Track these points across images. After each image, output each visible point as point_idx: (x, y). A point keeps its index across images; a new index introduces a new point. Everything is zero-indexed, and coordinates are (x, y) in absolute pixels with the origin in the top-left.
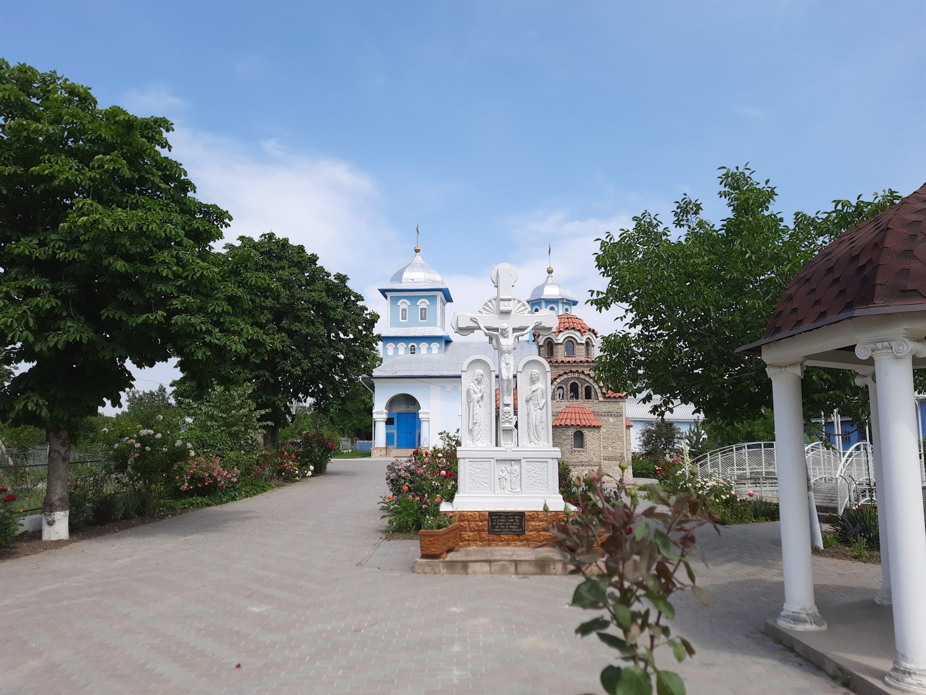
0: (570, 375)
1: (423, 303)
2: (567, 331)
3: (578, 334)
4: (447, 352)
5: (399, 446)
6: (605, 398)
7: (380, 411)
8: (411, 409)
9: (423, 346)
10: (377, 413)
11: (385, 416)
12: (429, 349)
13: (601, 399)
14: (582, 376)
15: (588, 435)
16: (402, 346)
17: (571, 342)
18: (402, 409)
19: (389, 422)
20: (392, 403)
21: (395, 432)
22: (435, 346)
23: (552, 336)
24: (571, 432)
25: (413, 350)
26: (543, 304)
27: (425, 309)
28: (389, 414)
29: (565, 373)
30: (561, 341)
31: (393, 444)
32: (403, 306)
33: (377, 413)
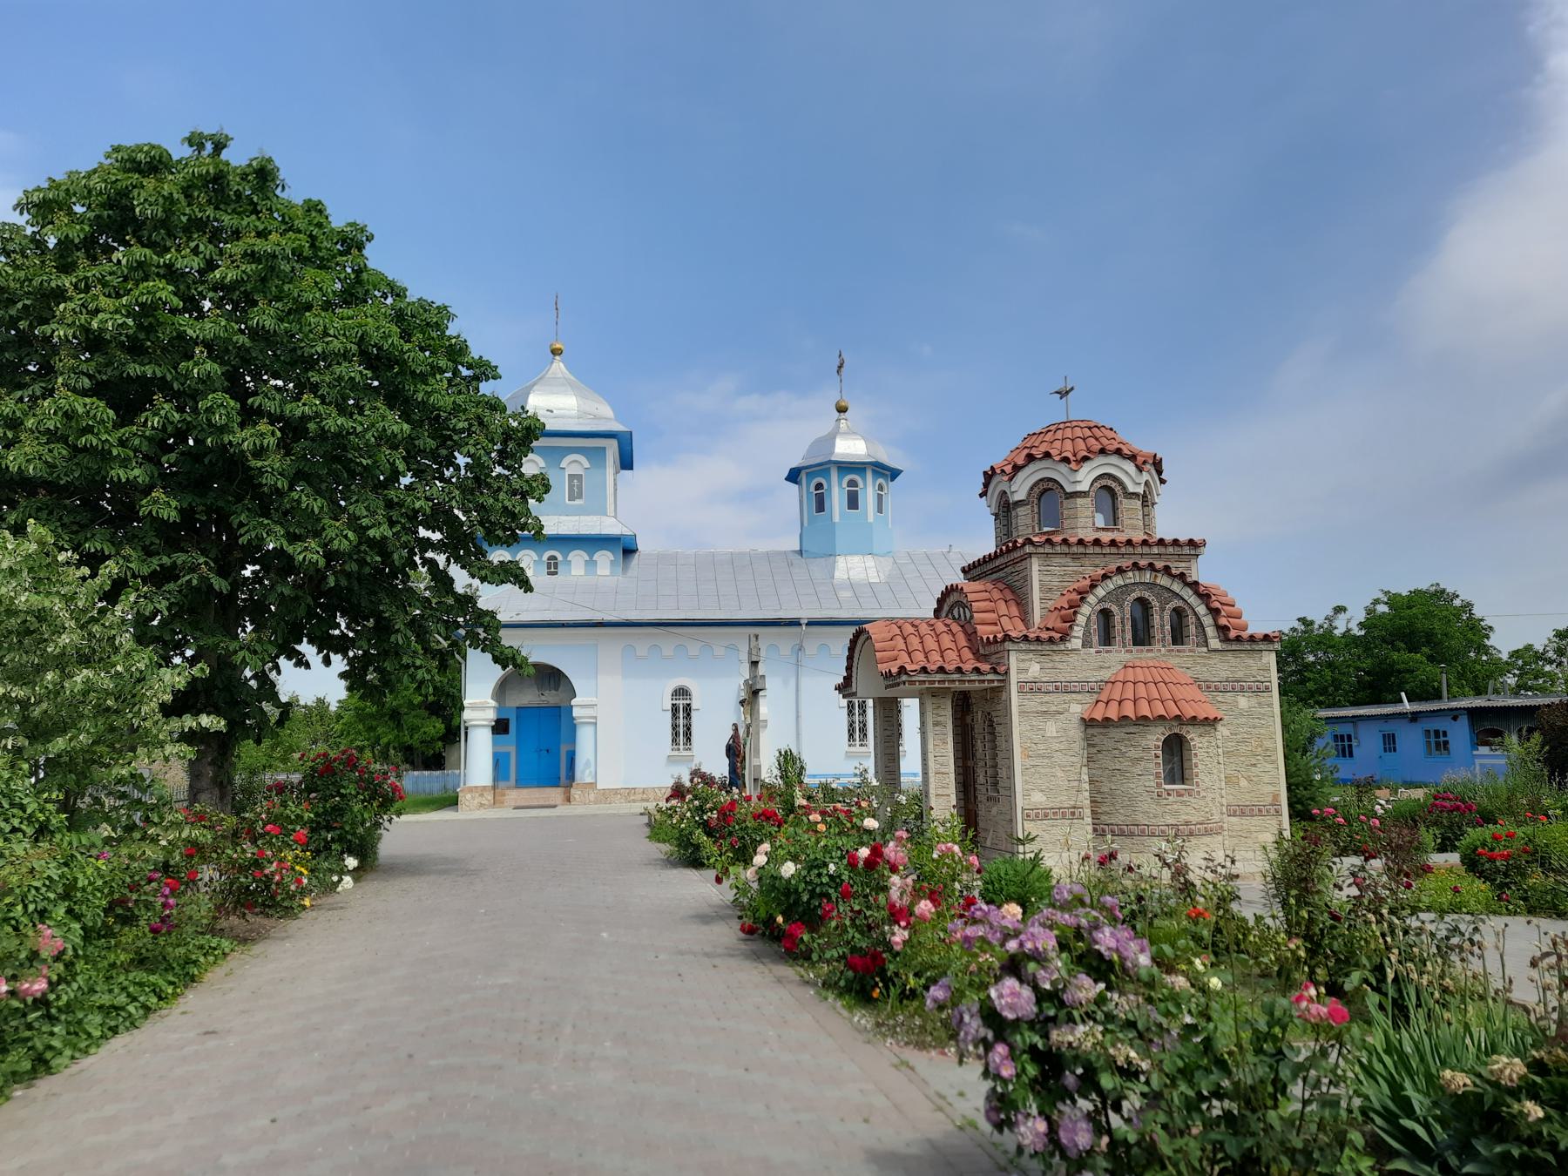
0: (1132, 577)
2: (1101, 460)
3: (1130, 467)
4: (630, 573)
5: (520, 784)
6: (1226, 640)
8: (551, 698)
9: (577, 557)
10: (474, 707)
11: (491, 715)
12: (591, 564)
13: (1215, 643)
14: (1163, 581)
15: (1197, 740)
17: (1109, 491)
19: (500, 727)
21: (512, 749)
22: (604, 558)
23: (1060, 473)
24: (1154, 738)
27: (579, 477)
28: (498, 710)
29: (1120, 571)
30: (1084, 487)
31: (507, 778)
33: (474, 707)
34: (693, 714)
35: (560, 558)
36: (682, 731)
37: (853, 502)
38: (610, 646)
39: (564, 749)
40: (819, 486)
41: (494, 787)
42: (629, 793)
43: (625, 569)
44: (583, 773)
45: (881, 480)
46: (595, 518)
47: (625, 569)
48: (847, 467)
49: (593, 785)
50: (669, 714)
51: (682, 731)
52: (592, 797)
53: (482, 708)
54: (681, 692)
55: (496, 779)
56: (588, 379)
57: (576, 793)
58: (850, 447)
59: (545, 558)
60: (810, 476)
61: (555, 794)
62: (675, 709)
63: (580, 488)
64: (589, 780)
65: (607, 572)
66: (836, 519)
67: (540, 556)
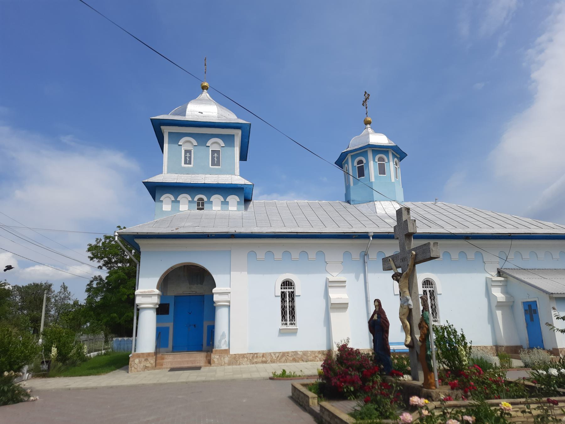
1: (215, 144)
4: (248, 210)
5: (176, 349)
7: (147, 290)
8: (197, 289)
9: (217, 199)
10: (143, 295)
11: (156, 300)
12: (225, 203)
16: (184, 198)
18: (183, 289)
19: (162, 310)
20: (166, 282)
21: (170, 325)
22: (233, 199)
25: (201, 205)
26: (370, 155)
28: (162, 297)
31: (166, 346)
32: (189, 147)
33: (143, 295)
34: (296, 299)
36: (288, 312)
37: (382, 170)
38: (239, 253)
39: (206, 324)
40: (360, 162)
41: (156, 353)
42: (253, 358)
43: (246, 208)
44: (220, 343)
45: (396, 159)
46: (228, 176)
47: (246, 208)
48: (378, 150)
49: (227, 351)
50: (279, 299)
51: (288, 312)
52: (227, 359)
53: (150, 295)
54: (287, 284)
55: (157, 347)
56: (221, 98)
57: (215, 357)
58: (379, 139)
59: (196, 199)
60: (353, 157)
61: (199, 358)
62: (283, 295)
63: (218, 158)
64: (224, 347)
65: (235, 209)
66: (373, 179)
67: (193, 198)
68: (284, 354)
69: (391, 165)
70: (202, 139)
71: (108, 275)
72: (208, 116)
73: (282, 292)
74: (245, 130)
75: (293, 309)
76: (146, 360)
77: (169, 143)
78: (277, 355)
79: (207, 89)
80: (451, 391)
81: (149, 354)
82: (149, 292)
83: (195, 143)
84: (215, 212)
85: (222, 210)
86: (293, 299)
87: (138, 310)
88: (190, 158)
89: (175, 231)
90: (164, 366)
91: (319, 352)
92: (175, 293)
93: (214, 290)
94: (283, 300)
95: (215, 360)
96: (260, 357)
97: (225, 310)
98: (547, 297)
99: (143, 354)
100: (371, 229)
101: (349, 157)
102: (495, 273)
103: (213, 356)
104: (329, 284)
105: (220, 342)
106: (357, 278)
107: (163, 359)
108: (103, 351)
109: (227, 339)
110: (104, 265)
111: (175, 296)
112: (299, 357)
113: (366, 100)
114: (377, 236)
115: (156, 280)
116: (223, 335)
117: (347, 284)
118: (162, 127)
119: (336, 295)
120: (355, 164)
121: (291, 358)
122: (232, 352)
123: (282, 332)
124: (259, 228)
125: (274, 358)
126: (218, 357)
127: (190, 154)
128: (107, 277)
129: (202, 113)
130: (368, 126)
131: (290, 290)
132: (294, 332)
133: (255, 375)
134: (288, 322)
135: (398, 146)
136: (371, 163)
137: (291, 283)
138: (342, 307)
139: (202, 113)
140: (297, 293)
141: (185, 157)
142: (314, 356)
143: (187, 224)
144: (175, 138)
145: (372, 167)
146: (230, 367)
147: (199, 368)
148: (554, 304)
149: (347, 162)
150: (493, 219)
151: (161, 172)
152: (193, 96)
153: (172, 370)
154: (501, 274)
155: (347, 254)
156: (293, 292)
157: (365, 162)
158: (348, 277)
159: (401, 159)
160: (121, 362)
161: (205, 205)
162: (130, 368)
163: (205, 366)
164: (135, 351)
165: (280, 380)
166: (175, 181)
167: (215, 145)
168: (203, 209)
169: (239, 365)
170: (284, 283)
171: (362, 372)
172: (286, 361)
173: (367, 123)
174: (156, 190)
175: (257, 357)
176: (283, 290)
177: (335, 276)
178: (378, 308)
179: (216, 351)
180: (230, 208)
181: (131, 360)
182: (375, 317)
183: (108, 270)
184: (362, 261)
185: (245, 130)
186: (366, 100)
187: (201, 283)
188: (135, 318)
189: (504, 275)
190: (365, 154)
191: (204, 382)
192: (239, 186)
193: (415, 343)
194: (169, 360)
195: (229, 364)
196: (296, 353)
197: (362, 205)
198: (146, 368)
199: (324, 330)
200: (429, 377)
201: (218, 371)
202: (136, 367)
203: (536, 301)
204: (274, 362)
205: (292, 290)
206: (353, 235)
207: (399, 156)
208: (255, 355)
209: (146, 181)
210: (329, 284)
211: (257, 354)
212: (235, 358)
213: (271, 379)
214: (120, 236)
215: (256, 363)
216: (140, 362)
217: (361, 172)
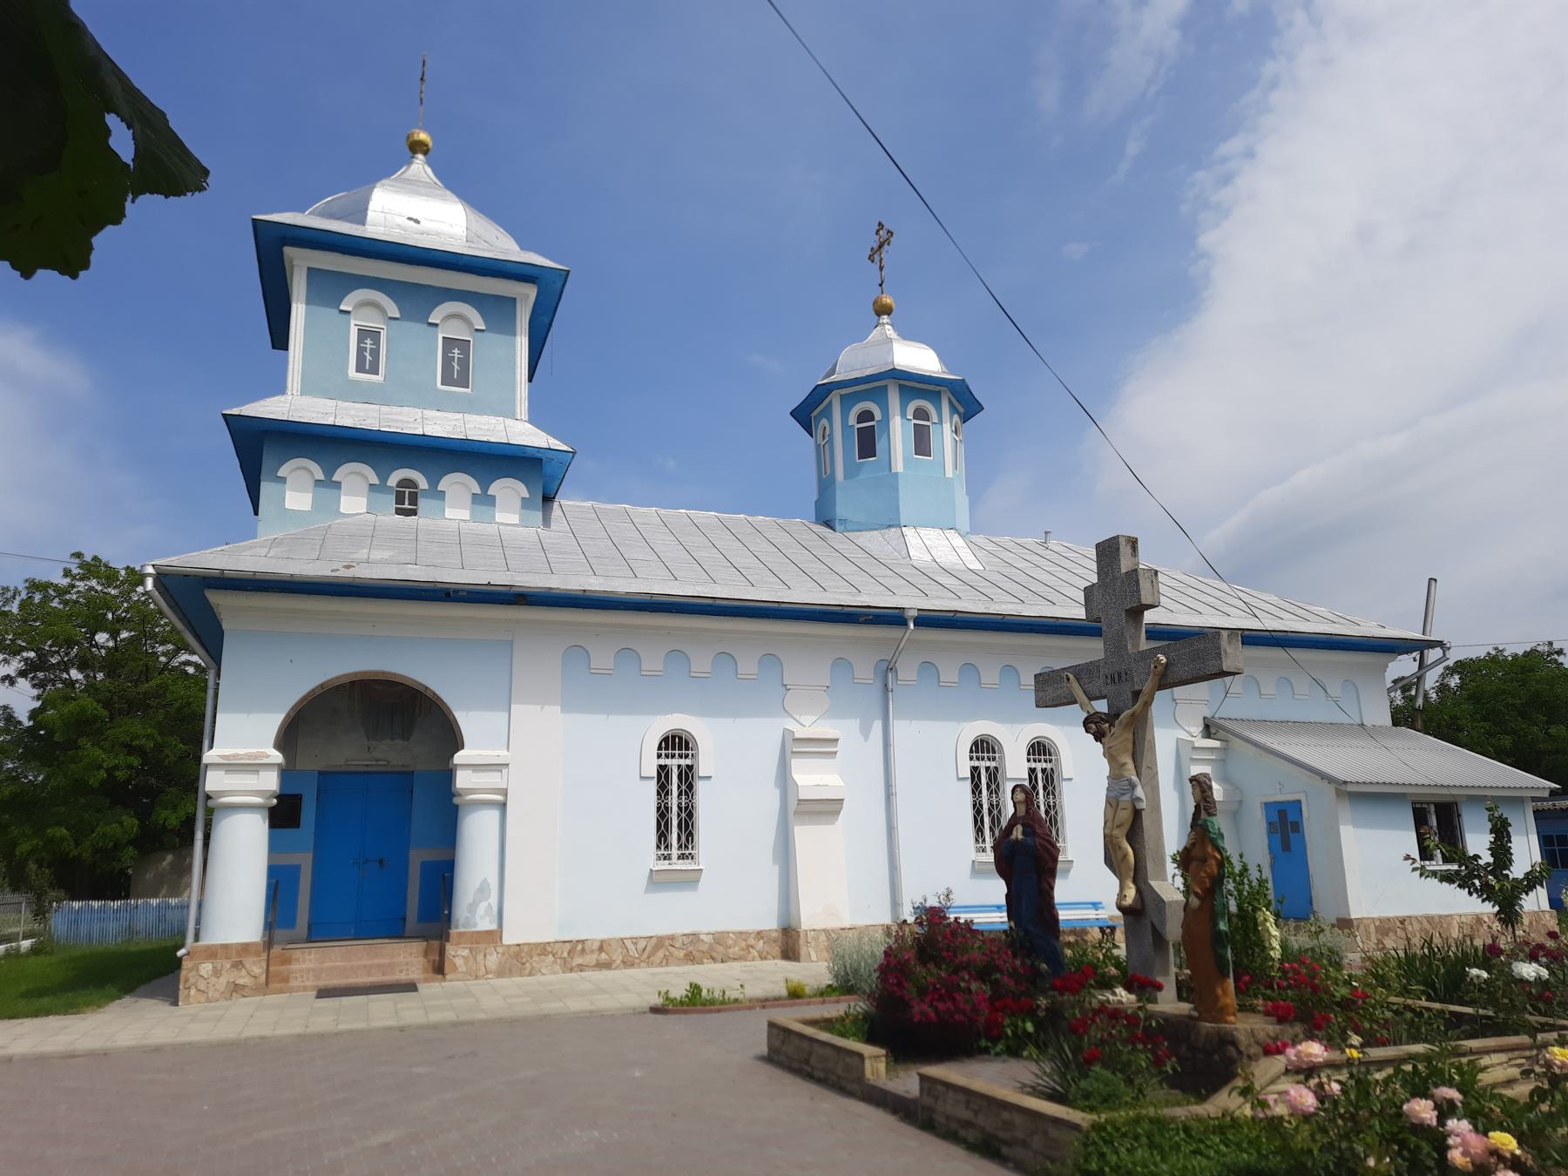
1: (454, 321)
5: (321, 931)
7: (243, 750)
8: (390, 754)
9: (459, 485)
10: (231, 767)
11: (270, 782)
12: (484, 500)
16: (355, 477)
19: (283, 814)
21: (304, 861)
22: (509, 491)
25: (407, 501)
27: (464, 345)
28: (285, 773)
33: (231, 767)
34: (701, 788)
35: (423, 484)
36: (676, 823)
37: (922, 443)
38: (539, 650)
39: (417, 858)
40: (866, 416)
41: (269, 943)
42: (571, 954)
46: (493, 420)
48: (913, 385)
49: (494, 937)
50: (652, 786)
51: (676, 823)
52: (493, 960)
53: (253, 767)
55: (270, 926)
57: (457, 954)
58: (918, 358)
59: (393, 481)
60: (847, 402)
61: (406, 957)
63: (464, 363)
64: (485, 924)
66: (899, 466)
67: (384, 477)
68: (661, 942)
69: (945, 433)
70: (416, 303)
71: (38, 704)
72: (438, 234)
73: (662, 768)
74: (549, 288)
75: (690, 815)
76: (238, 965)
77: (308, 303)
78: (642, 944)
79: (425, 153)
80: (1278, 1027)
81: (245, 948)
82: (249, 756)
83: (394, 311)
84: (455, 525)
85: (474, 519)
86: (690, 787)
87: (210, 812)
88: (375, 353)
89: (344, 573)
90: (293, 983)
91: (759, 933)
92: (321, 765)
93: (459, 757)
94: (663, 789)
95: (459, 962)
96: (592, 951)
97: (490, 817)
98: (1330, 790)
99: (225, 947)
100: (911, 601)
101: (835, 399)
102: (1197, 729)
103: (450, 949)
104: (792, 748)
105: (473, 908)
106: (866, 732)
107: (288, 961)
108: (26, 944)
109: (494, 900)
110: (22, 674)
111: (320, 773)
112: (704, 948)
113: (881, 246)
114: (929, 620)
115: (272, 722)
116: (483, 890)
117: (839, 748)
118: (289, 251)
119: (811, 778)
120: (852, 420)
121: (681, 954)
122: (508, 939)
123: (657, 881)
124: (601, 580)
125: (633, 952)
126: (466, 952)
127: (377, 342)
128: (34, 714)
129: (417, 222)
130: (885, 319)
131: (683, 762)
132: (691, 880)
133: (606, 1003)
134: (675, 852)
135: (968, 382)
136: (896, 423)
137: (687, 743)
138: (827, 809)
139: (417, 222)
140: (703, 769)
141: (361, 351)
142: (743, 944)
143: (377, 555)
144: (329, 288)
145: (899, 432)
146: (505, 981)
147: (411, 987)
148: (1345, 810)
149: (827, 413)
150: (1190, 591)
151: (280, 389)
152: (384, 168)
153: (324, 993)
154: (1213, 730)
155: (841, 664)
156: (690, 767)
157: (878, 416)
158: (843, 729)
159: (965, 418)
160: (152, 969)
161: (423, 503)
162: (182, 994)
163: (426, 980)
164: (197, 938)
165: (685, 1012)
166: (330, 421)
167: (455, 323)
168: (413, 513)
169: (530, 974)
170: (666, 739)
171: (995, 985)
172: (666, 961)
173: (882, 310)
174: (260, 447)
175: (583, 950)
176: (663, 762)
177: (809, 725)
178: (1022, 810)
179: (461, 934)
180: (499, 517)
181: (186, 964)
182: (1018, 833)
183: (35, 692)
184: (879, 685)
185: (549, 288)
186: (881, 246)
187: (406, 735)
188: (199, 836)
189: (1222, 734)
190: (879, 394)
191: (455, 1024)
192: (530, 453)
193: (1148, 901)
194: (311, 966)
195: (501, 973)
196: (694, 937)
197: (868, 534)
198: (236, 989)
199: (772, 874)
200: (1219, 991)
201: (468, 994)
202: (202, 986)
203: (1299, 802)
204: (632, 965)
205: (688, 762)
206: (861, 615)
207: (961, 410)
208: (577, 947)
209: (235, 411)
210: (792, 748)
211: (583, 942)
212: (517, 956)
213: (655, 1010)
214: (162, 578)
215: (581, 968)
216: (217, 973)
217: (867, 444)
